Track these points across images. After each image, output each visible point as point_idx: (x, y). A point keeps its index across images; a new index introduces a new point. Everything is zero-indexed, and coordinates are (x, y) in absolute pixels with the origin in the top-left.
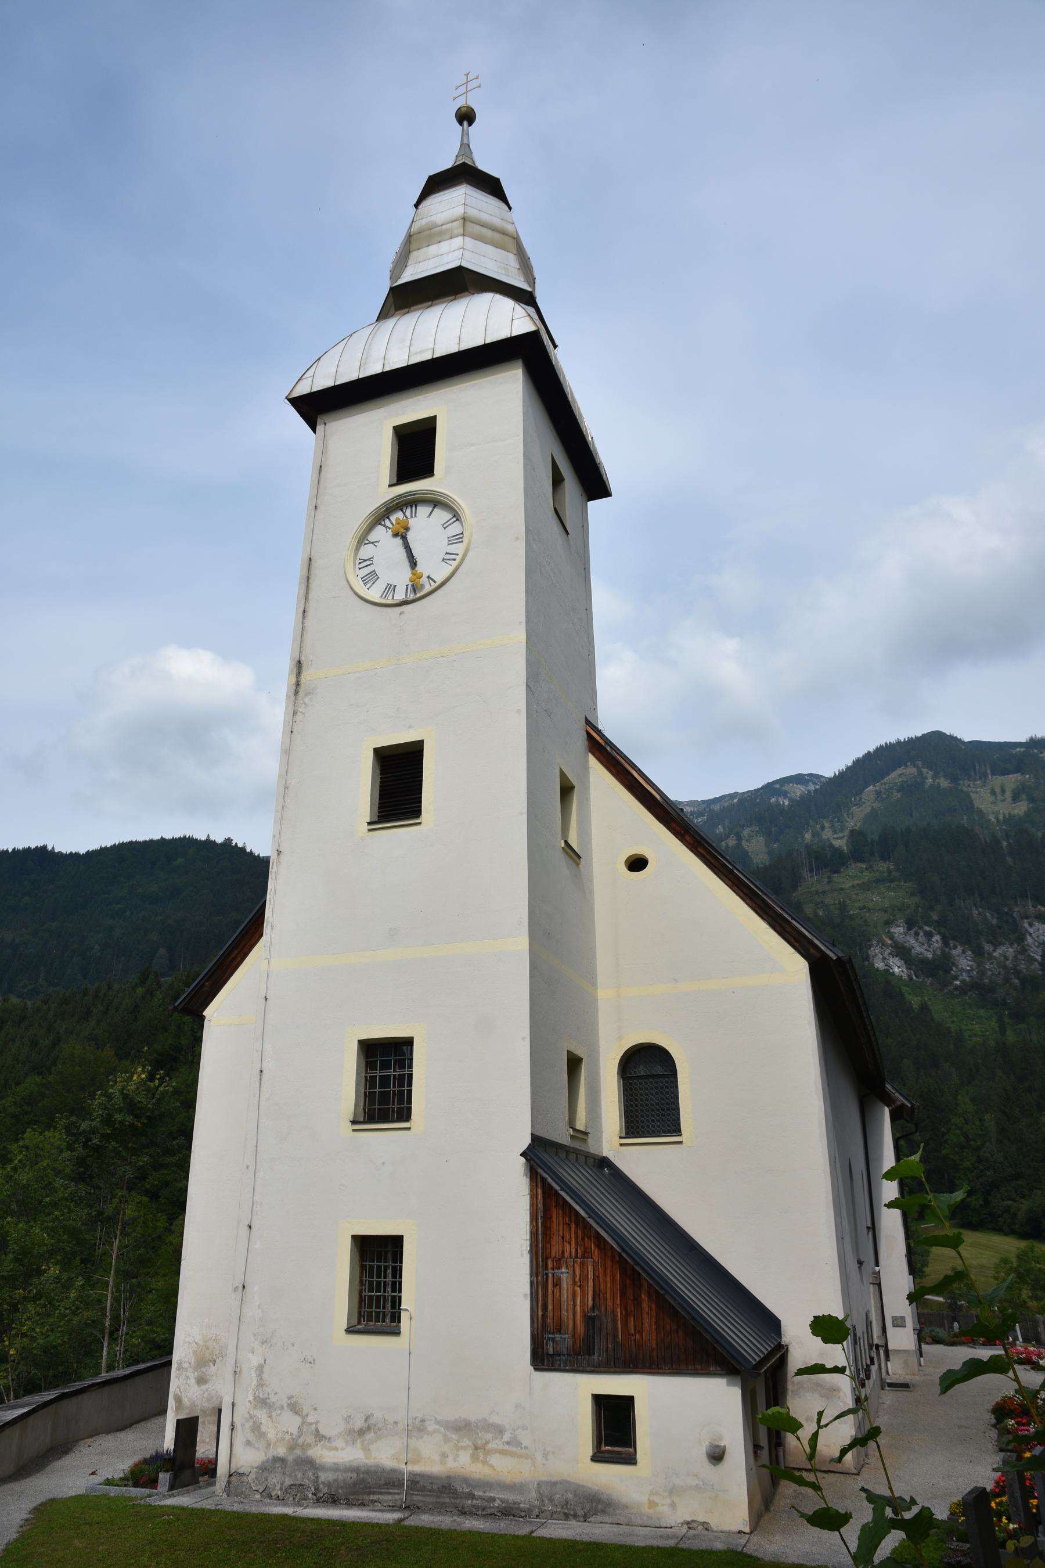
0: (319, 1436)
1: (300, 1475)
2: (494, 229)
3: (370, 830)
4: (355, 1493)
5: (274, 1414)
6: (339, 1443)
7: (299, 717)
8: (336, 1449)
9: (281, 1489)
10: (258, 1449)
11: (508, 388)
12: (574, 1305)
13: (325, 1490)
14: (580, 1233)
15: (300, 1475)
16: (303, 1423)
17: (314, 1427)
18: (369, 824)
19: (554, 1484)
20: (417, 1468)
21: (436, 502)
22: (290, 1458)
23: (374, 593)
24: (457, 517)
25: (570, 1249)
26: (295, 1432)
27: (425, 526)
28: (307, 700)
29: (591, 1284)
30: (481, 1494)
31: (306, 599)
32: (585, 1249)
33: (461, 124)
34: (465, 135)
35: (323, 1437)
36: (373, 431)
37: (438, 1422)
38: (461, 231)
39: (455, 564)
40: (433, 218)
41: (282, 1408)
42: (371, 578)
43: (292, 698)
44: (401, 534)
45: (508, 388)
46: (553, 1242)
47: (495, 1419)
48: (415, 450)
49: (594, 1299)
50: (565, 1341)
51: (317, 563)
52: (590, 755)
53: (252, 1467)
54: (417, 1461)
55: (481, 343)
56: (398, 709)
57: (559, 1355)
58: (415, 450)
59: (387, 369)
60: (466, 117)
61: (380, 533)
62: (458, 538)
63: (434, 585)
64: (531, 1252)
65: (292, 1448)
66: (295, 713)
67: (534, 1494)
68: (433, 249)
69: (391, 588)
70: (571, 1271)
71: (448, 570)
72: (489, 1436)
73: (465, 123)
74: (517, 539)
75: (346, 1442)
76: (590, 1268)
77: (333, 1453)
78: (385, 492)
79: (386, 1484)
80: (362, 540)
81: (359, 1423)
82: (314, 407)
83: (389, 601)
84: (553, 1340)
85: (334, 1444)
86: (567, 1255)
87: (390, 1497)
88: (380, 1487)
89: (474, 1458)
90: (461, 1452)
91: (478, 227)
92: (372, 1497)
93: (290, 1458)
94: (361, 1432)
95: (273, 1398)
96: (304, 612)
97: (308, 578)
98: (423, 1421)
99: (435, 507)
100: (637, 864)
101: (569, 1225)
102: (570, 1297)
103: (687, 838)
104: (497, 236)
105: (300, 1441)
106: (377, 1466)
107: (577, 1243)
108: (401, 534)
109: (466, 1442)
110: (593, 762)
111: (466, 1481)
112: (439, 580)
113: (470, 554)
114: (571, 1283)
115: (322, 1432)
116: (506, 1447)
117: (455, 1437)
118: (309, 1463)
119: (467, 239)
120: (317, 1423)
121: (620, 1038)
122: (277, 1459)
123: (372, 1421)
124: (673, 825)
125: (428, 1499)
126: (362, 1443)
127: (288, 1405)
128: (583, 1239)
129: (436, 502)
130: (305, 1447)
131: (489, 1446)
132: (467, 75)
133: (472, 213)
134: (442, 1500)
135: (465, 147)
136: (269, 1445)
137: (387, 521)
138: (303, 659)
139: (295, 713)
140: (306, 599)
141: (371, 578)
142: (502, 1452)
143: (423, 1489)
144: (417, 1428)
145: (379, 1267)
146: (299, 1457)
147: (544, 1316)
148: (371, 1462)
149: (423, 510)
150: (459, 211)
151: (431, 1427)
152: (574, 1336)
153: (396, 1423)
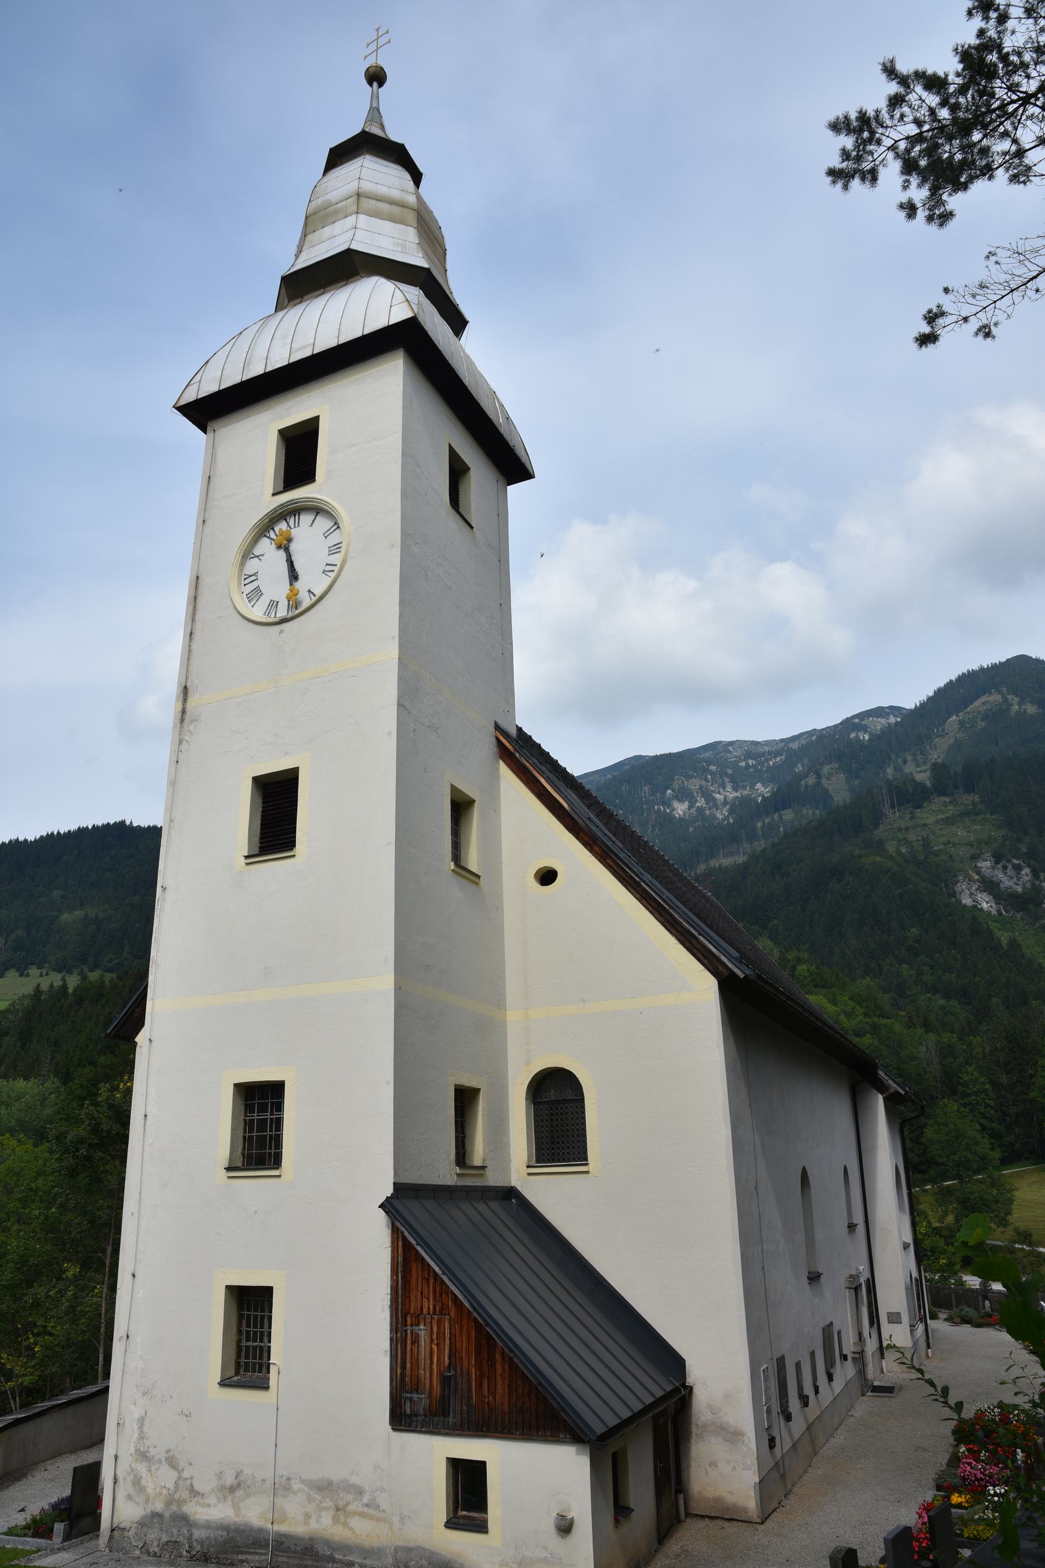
0: (194, 1492)
1: (175, 1531)
2: (392, 202)
3: (247, 864)
4: (224, 1553)
5: (153, 1468)
6: (212, 1500)
7: (184, 746)
8: (209, 1506)
9: (158, 1545)
10: (138, 1504)
11: (391, 378)
12: (431, 1364)
13: (198, 1548)
14: (438, 1288)
15: (175, 1531)
16: (180, 1477)
17: (189, 1481)
18: (246, 857)
19: (409, 1550)
20: (282, 1528)
21: (318, 510)
22: (167, 1514)
23: (258, 612)
24: (337, 525)
25: (428, 1305)
26: (171, 1485)
27: (307, 535)
28: (191, 728)
29: (447, 1342)
30: (341, 1557)
31: (193, 620)
32: (443, 1305)
33: (371, 85)
34: (375, 97)
35: (198, 1493)
36: (258, 434)
37: (302, 1481)
38: (354, 208)
39: (333, 575)
40: (328, 197)
41: (160, 1462)
42: (255, 595)
43: (179, 726)
44: (285, 545)
45: (391, 378)
46: (413, 1298)
47: (355, 1480)
48: (299, 454)
49: (450, 1358)
50: (422, 1400)
51: (205, 581)
52: (501, 762)
53: (132, 1522)
54: (282, 1522)
55: (359, 334)
56: (275, 735)
57: (416, 1416)
58: (299, 454)
59: (269, 369)
60: (376, 77)
61: (265, 546)
62: (336, 549)
63: (314, 599)
64: (391, 1307)
65: (168, 1504)
66: (181, 742)
67: (390, 1560)
68: (327, 231)
69: (274, 604)
70: (429, 1328)
71: (327, 581)
72: (350, 1497)
73: (375, 84)
74: (393, 546)
75: (218, 1499)
76: (447, 1325)
77: (205, 1510)
78: (269, 503)
79: (254, 1544)
80: (248, 553)
81: (230, 1480)
82: (206, 412)
83: (269, 620)
84: (411, 1399)
85: (207, 1501)
86: (425, 1311)
87: (257, 1558)
88: (248, 1546)
89: (336, 1520)
90: (324, 1513)
91: (373, 202)
92: (241, 1557)
93: (167, 1514)
94: (232, 1489)
95: (152, 1452)
96: (191, 634)
97: (195, 598)
98: (289, 1479)
99: (317, 514)
100: (547, 877)
101: (428, 1280)
102: (428, 1355)
103: (596, 848)
104: (396, 210)
105: (176, 1496)
106: (246, 1525)
107: (435, 1299)
108: (285, 545)
109: (328, 1503)
110: (504, 769)
111: (328, 1543)
112: (318, 592)
113: (348, 564)
114: (428, 1341)
115: (196, 1487)
116: (365, 1509)
117: (318, 1497)
118: (183, 1520)
119: (361, 216)
120: (192, 1478)
121: (528, 1063)
122: (155, 1515)
123: (242, 1478)
124: (582, 835)
125: (291, 1561)
126: (233, 1500)
127: (166, 1459)
128: (441, 1294)
129: (318, 510)
130: (181, 1503)
131: (350, 1508)
132: (378, 30)
133: (367, 186)
134: (304, 1563)
135: (375, 114)
136: (148, 1500)
137: (272, 532)
138: (189, 684)
139: (181, 742)
140: (193, 620)
141: (255, 595)
142: (362, 1515)
143: (287, 1550)
144: (281, 1487)
145: (256, 1316)
146: (175, 1513)
147: (403, 1375)
148: (239, 1520)
149: (306, 519)
150: (353, 187)
151: (296, 1485)
152: (430, 1396)
153: (264, 1480)
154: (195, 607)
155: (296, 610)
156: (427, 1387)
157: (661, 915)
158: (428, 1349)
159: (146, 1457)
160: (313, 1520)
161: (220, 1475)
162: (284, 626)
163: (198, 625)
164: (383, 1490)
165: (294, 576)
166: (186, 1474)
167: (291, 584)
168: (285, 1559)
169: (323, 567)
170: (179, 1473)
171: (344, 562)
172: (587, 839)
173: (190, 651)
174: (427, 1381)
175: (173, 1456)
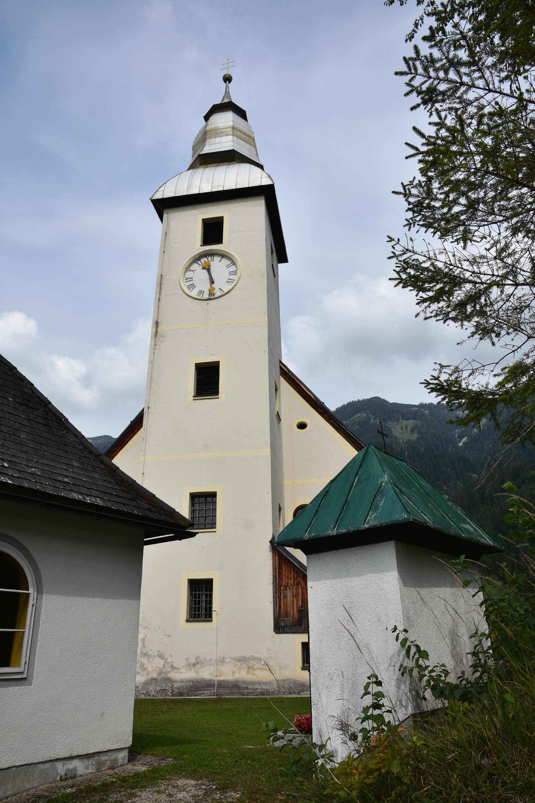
0: (173, 668)
1: (164, 685)
2: (245, 134)
3: (194, 400)
4: (191, 691)
5: (151, 659)
6: (183, 670)
7: (157, 347)
8: (182, 673)
9: (155, 692)
10: (143, 675)
11: (257, 208)
12: (293, 606)
13: (177, 691)
14: (295, 575)
15: (164, 685)
16: (165, 662)
17: (171, 664)
18: (194, 397)
19: (284, 681)
20: (221, 678)
21: (223, 255)
22: (159, 678)
23: (194, 293)
24: (233, 263)
25: (291, 582)
26: (161, 666)
28: (161, 339)
29: (301, 596)
30: (251, 687)
31: (160, 293)
32: (298, 582)
33: (225, 82)
34: (227, 87)
35: (175, 668)
36: (192, 220)
37: (230, 658)
38: (231, 133)
39: (233, 284)
40: (217, 125)
41: (155, 656)
42: (192, 287)
43: (154, 338)
44: (208, 269)
45: (257, 208)
46: (283, 579)
47: (257, 655)
48: (213, 231)
49: (302, 603)
50: (289, 620)
51: (166, 277)
52: (281, 377)
53: (140, 683)
54: (221, 675)
55: (247, 186)
56: (207, 347)
57: (286, 627)
58: (213, 231)
59: (201, 192)
60: (228, 79)
61: (195, 266)
62: (235, 273)
63: (223, 293)
64: (273, 584)
65: (160, 674)
66: (155, 345)
67: (276, 685)
68: (218, 139)
69: (201, 292)
70: (292, 591)
71: (229, 287)
72: (255, 663)
73: (227, 82)
74: (263, 276)
75: (187, 670)
76: (300, 589)
77: (180, 675)
78: (198, 248)
79: (206, 686)
80: (187, 269)
81: (193, 661)
83: (201, 297)
84: (284, 620)
85: (181, 671)
86: (290, 584)
87: (208, 692)
88: (204, 687)
89: (248, 672)
90: (242, 670)
91: (238, 132)
92: (200, 692)
93: (159, 678)
94: (194, 665)
95: (150, 652)
96: (159, 299)
97: (161, 284)
98: (224, 658)
99: (222, 257)
100: (302, 426)
101: (290, 572)
102: (291, 602)
103: (325, 415)
104: (247, 138)
105: (164, 670)
106: (202, 679)
107: (294, 579)
108: (208, 269)
109: (244, 666)
110: (282, 380)
111: (244, 682)
112: (226, 291)
113: (241, 280)
114: (291, 596)
115: (175, 665)
116: (263, 667)
117: (239, 664)
118: (170, 680)
119: (234, 137)
120: (172, 662)
121: (294, 502)
122: (152, 679)
123: (199, 659)
124: (319, 409)
125: (226, 691)
126: (195, 669)
127: (158, 655)
128: (297, 578)
129: (223, 255)
130: (166, 673)
131: (255, 667)
132: (228, 60)
133: (237, 126)
134: (233, 691)
135: (227, 93)
136: (148, 673)
137: (199, 262)
138: (159, 320)
139: (155, 345)
140: (160, 293)
141: (192, 287)
142: (261, 669)
143: (224, 687)
144: (222, 661)
145: (199, 594)
146: (163, 677)
147: (280, 610)
148: (199, 677)
149: (217, 259)
150: (231, 124)
151: (227, 660)
152: (293, 618)
153: (211, 660)
154: (161, 288)
155: (212, 297)
156: (292, 615)
157: (354, 444)
158: (292, 600)
159: (147, 655)
160: (237, 673)
161: (187, 659)
162: (209, 302)
163: (163, 297)
164: (271, 658)
165: (212, 282)
166: (169, 661)
167: (211, 285)
168: (223, 691)
169: (227, 280)
170: (165, 660)
171: (239, 279)
172: (321, 411)
173: (159, 307)
174: (292, 613)
175: (162, 654)
